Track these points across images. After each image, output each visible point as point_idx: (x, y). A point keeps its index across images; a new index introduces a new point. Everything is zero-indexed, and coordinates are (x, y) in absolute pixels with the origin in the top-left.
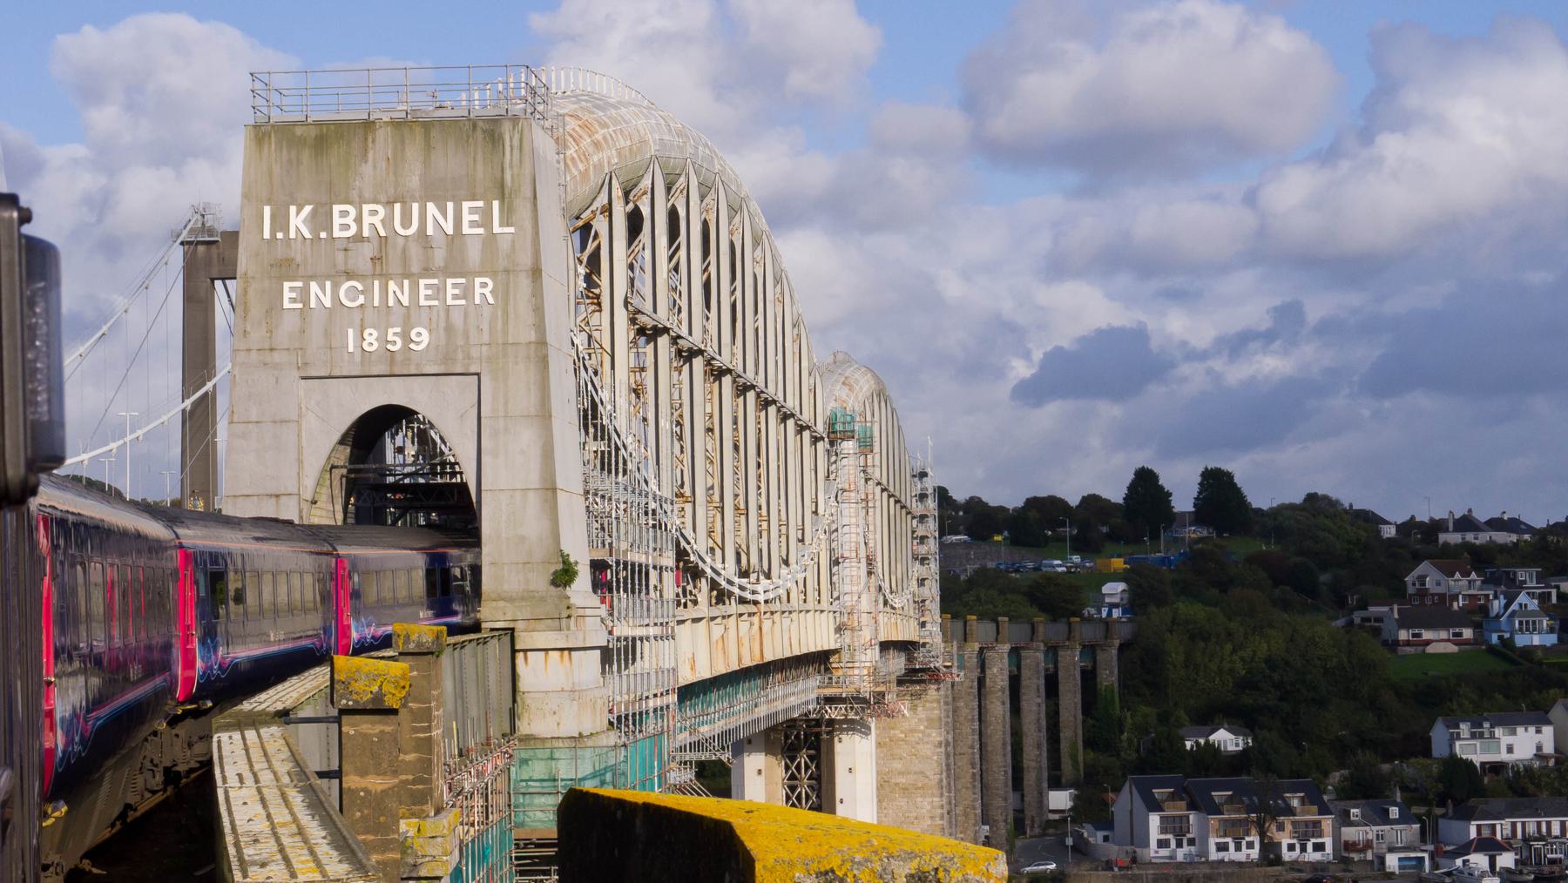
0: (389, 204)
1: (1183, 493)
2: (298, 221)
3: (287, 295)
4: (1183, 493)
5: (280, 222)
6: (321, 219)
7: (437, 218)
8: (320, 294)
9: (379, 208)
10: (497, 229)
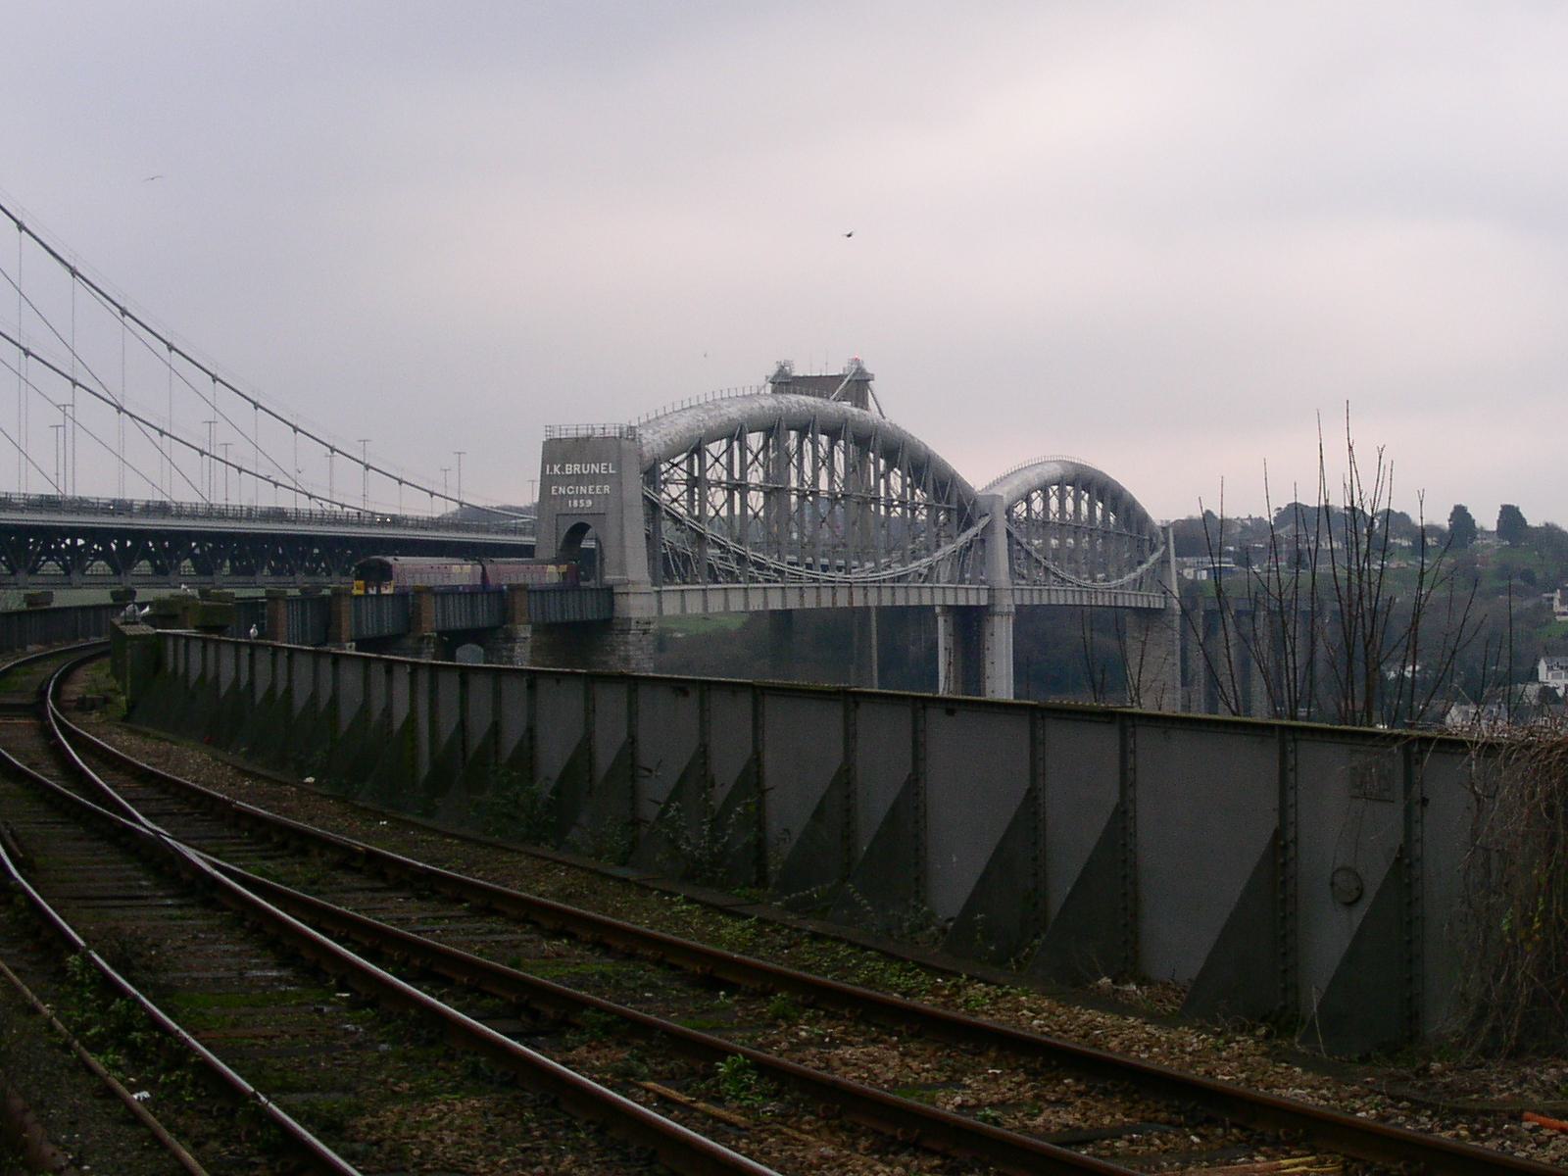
0: (581, 464)
1: (1487, 519)
2: (556, 469)
3: (553, 491)
4: (1487, 519)
5: (552, 469)
6: (562, 469)
7: (594, 468)
8: (562, 490)
9: (579, 465)
10: (611, 471)
